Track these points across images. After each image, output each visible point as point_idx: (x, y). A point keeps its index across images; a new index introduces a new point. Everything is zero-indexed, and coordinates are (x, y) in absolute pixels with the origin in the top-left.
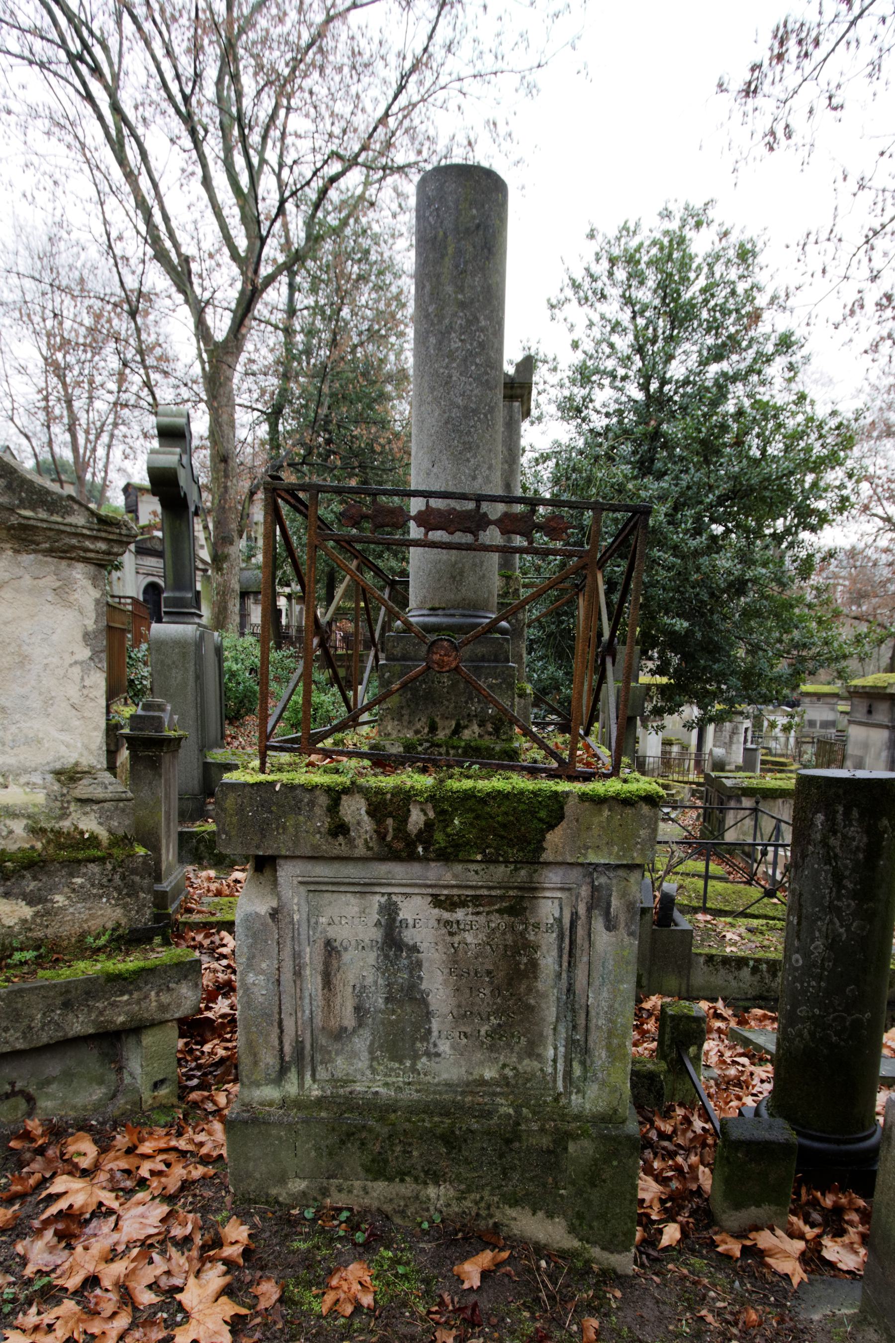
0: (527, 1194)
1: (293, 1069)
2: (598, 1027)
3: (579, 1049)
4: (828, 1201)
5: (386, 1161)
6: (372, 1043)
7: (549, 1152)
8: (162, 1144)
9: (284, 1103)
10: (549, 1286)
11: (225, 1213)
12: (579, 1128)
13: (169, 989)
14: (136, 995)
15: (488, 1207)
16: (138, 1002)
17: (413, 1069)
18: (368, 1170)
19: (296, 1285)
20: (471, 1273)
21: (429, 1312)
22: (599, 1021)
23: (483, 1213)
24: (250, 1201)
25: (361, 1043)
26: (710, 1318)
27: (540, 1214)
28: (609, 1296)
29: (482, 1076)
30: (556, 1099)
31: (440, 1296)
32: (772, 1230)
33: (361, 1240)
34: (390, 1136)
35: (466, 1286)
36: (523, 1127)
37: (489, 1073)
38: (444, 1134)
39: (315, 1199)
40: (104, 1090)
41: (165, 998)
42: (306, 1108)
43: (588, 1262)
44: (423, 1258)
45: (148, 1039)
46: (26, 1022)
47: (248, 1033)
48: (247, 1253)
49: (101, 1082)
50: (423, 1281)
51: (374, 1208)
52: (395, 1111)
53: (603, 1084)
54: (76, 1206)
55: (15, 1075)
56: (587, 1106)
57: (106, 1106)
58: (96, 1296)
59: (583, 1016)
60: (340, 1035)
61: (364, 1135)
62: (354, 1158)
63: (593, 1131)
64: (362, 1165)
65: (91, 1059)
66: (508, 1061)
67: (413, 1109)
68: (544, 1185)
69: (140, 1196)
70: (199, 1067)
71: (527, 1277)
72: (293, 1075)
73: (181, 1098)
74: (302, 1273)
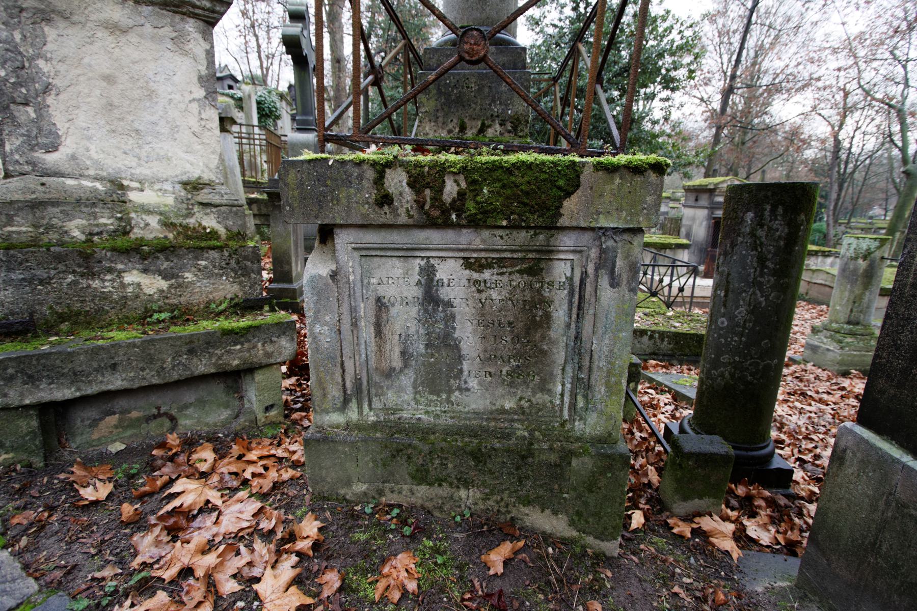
0: (537, 497)
1: (354, 400)
2: (600, 368)
3: (582, 385)
4: (741, 491)
5: (427, 471)
6: (415, 381)
7: (556, 465)
8: (265, 453)
9: (348, 426)
10: (560, 569)
11: (304, 509)
12: (581, 447)
13: (271, 342)
14: (246, 345)
15: (507, 506)
16: (249, 350)
17: (448, 401)
18: (413, 478)
19: (355, 574)
20: (496, 559)
21: (463, 600)
22: (601, 363)
23: (503, 510)
24: (325, 499)
25: (407, 380)
26: (683, 595)
27: (548, 512)
28: (603, 576)
29: (503, 406)
30: (563, 425)
31: (471, 581)
32: (711, 516)
33: (408, 533)
34: (431, 452)
35: (492, 572)
36: (536, 446)
37: (509, 404)
38: (474, 451)
39: (374, 498)
40: (229, 412)
41: (269, 348)
42: (365, 430)
43: (584, 547)
44: (456, 547)
45: (259, 376)
46: (159, 364)
47: (318, 372)
48: (316, 546)
49: (227, 406)
50: (457, 568)
51: (418, 505)
52: (433, 433)
53: (601, 413)
54: (185, 505)
55: (159, 402)
56: (588, 430)
57: (231, 423)
58: (189, 585)
59: (588, 359)
60: (390, 374)
61: (410, 451)
62: (403, 469)
63: (592, 450)
64: (409, 474)
65: (218, 390)
66: (524, 395)
67: (448, 432)
68: (551, 490)
69: (242, 494)
70: (303, 396)
71: (539, 563)
72: (353, 405)
73: (287, 416)
74: (360, 562)
